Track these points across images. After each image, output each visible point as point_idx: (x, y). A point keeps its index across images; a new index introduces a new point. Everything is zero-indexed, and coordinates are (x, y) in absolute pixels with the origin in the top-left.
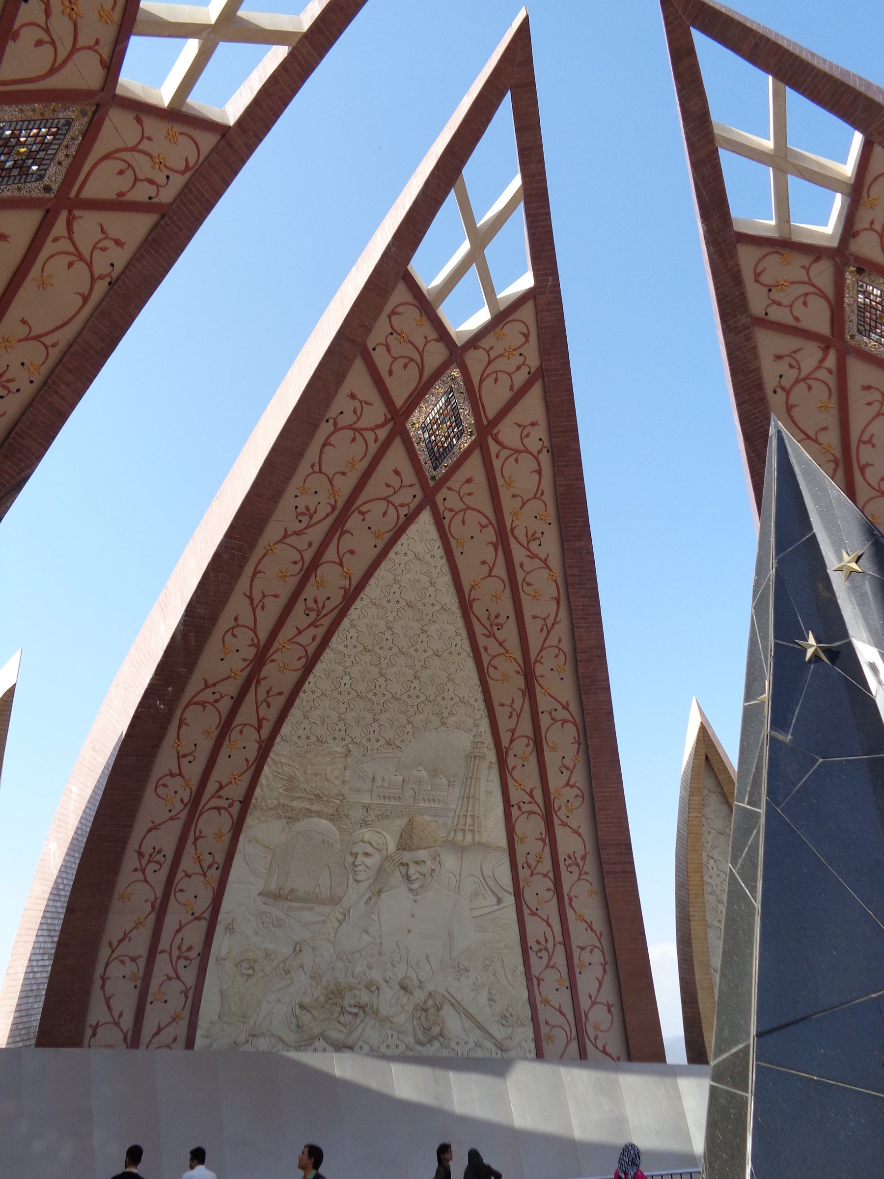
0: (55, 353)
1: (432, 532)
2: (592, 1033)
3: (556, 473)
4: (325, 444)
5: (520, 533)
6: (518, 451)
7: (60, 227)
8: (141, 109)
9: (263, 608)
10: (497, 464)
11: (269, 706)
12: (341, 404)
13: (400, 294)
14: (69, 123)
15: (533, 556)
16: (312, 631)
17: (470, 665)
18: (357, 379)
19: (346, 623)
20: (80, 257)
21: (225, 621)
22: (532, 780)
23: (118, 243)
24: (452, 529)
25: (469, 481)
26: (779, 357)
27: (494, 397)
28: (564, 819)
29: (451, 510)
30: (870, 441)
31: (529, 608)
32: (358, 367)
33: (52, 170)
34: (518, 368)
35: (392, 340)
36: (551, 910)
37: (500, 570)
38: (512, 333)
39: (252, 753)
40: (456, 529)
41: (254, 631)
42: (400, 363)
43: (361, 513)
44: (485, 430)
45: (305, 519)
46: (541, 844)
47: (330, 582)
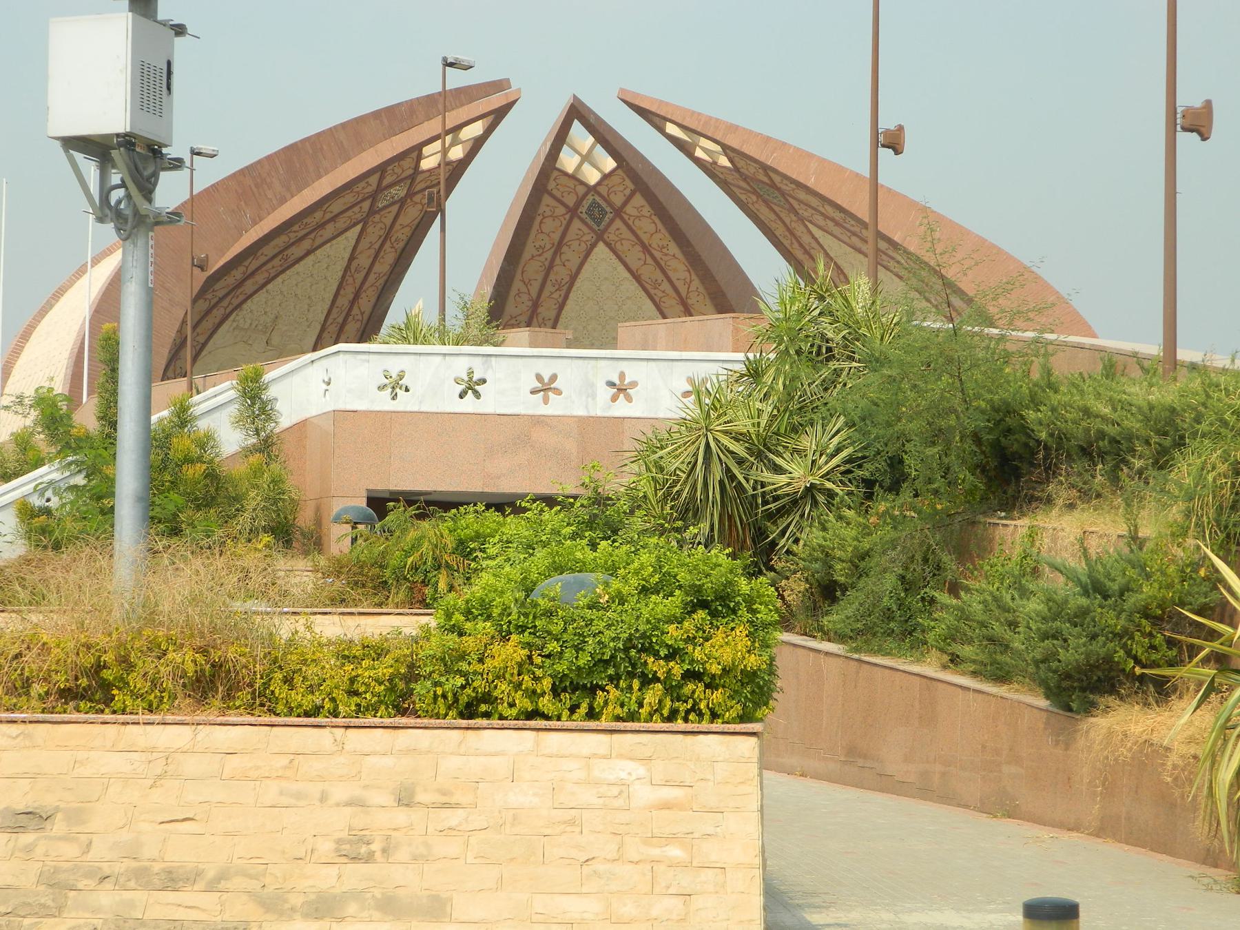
1: (607, 250)
3: (664, 223)
4: (541, 222)
5: (654, 245)
8: (429, 171)
10: (630, 222)
12: (542, 208)
13: (555, 173)
17: (649, 302)
18: (547, 200)
19: (574, 288)
21: (513, 292)
27: (618, 200)
37: (649, 260)
38: (616, 179)
40: (618, 246)
44: (618, 212)
47: (560, 273)
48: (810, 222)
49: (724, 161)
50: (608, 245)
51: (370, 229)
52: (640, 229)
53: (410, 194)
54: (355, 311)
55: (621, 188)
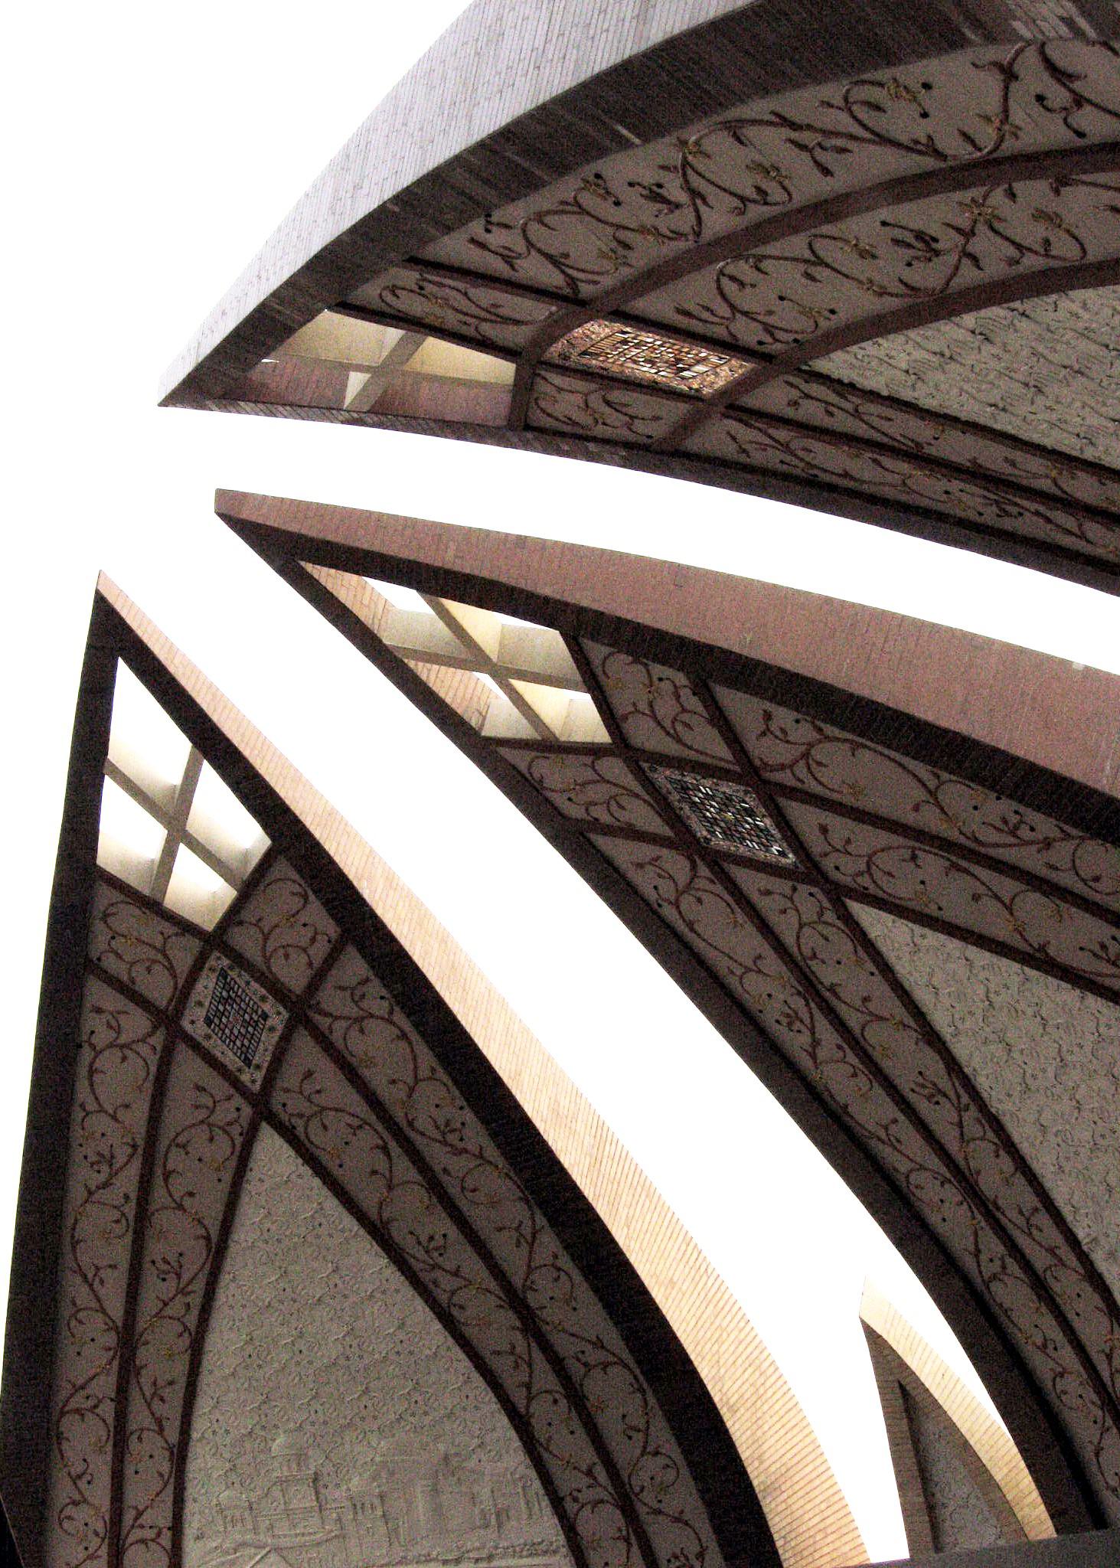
1: (287, 1152)
9: (102, 1282)
11: (162, 1399)
18: (97, 992)
22: (588, 1456)
24: (312, 1137)
25: (309, 1074)
28: (656, 1505)
29: (301, 1116)
30: (814, 956)
31: (481, 1218)
40: (317, 1136)
41: (103, 1311)
43: (177, 1145)
44: (301, 1011)
46: (622, 1546)
47: (177, 1238)
49: (571, 712)
55: (303, 937)
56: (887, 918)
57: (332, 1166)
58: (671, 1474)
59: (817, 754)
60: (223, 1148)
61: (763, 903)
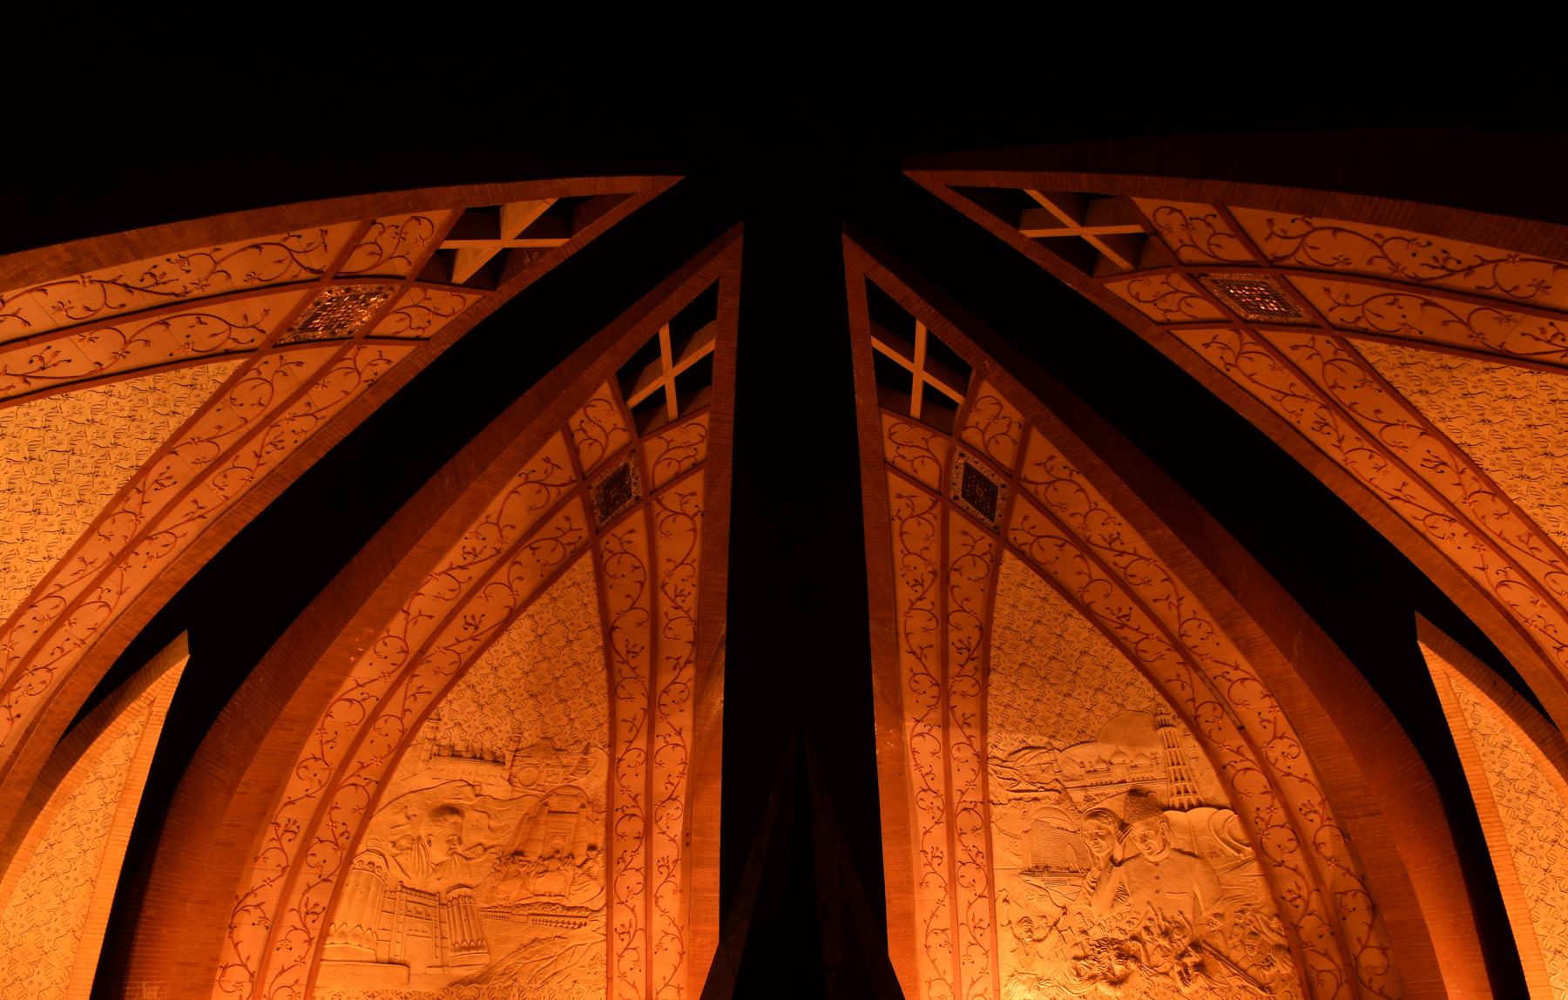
0: (696, 565)
1: (1021, 565)
2: (1366, 978)
4: (902, 534)
5: (1096, 539)
6: (1050, 483)
7: (658, 508)
10: (1041, 497)
12: (896, 504)
14: (626, 466)
15: (1122, 553)
16: (971, 665)
19: (993, 652)
20: (675, 513)
21: (906, 676)
22: (1239, 741)
23: (693, 494)
25: (1026, 518)
26: (1207, 345)
27: (1004, 453)
31: (1144, 592)
32: (893, 479)
33: (633, 489)
34: (1009, 426)
35: (901, 451)
36: (1297, 859)
37: (1097, 572)
39: (974, 764)
40: (1039, 556)
42: (917, 463)
45: (919, 588)
46: (1268, 798)
48: (1366, 334)
50: (1020, 554)
51: (611, 567)
52: (1063, 507)
53: (654, 492)
54: (662, 728)
56: (1383, 347)
57: (1051, 569)
58: (1294, 751)
59: (1310, 240)
60: (981, 570)
61: (1294, 356)
